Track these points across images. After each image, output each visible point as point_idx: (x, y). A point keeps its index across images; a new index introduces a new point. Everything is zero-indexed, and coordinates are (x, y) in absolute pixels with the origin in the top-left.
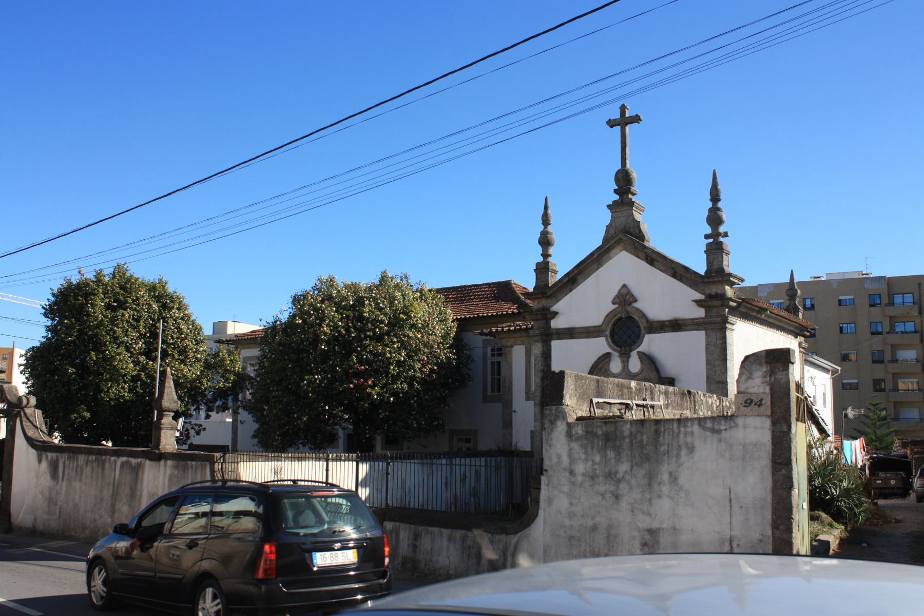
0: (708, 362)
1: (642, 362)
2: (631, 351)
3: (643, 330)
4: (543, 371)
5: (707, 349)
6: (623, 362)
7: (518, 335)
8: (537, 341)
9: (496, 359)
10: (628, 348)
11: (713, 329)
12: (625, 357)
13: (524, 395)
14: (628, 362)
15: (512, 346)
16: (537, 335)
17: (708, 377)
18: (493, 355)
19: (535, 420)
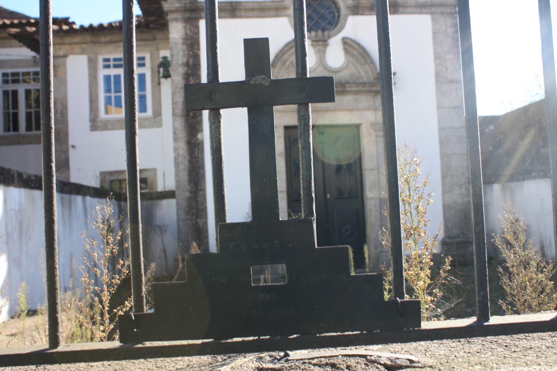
0: (437, 56)
1: (346, 51)
2: (329, 37)
3: (343, 11)
4: (187, 64)
5: (434, 38)
6: (317, 52)
7: (77, 39)
8: (176, 20)
9: (11, 87)
10: (326, 33)
11: (442, 13)
12: (322, 43)
13: (87, 124)
14: (324, 52)
15: (65, 56)
16: (177, 11)
17: (437, 75)
18: (6, 82)
19: (175, 140)
